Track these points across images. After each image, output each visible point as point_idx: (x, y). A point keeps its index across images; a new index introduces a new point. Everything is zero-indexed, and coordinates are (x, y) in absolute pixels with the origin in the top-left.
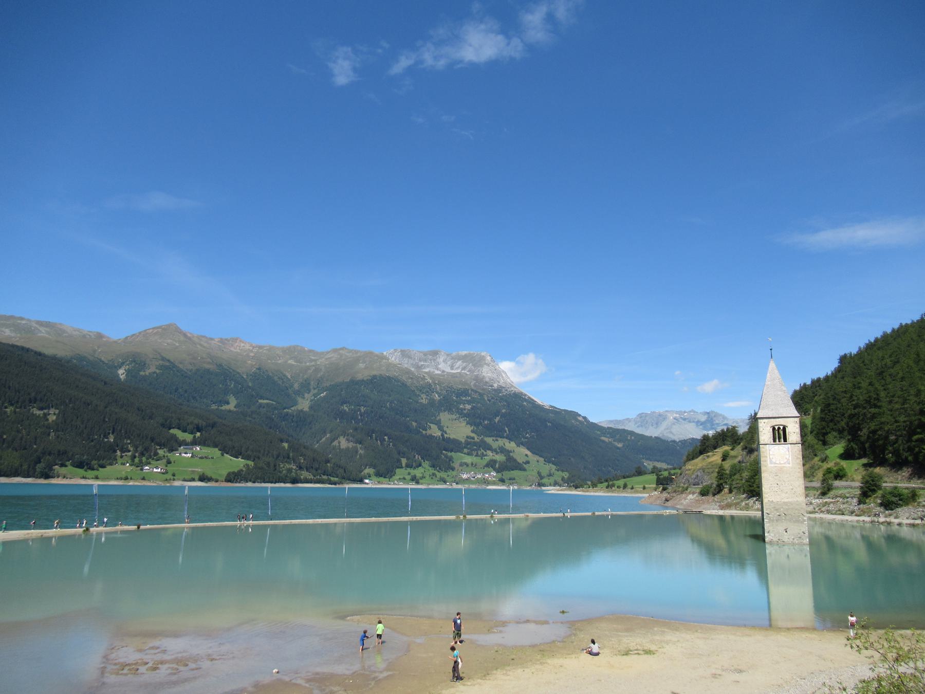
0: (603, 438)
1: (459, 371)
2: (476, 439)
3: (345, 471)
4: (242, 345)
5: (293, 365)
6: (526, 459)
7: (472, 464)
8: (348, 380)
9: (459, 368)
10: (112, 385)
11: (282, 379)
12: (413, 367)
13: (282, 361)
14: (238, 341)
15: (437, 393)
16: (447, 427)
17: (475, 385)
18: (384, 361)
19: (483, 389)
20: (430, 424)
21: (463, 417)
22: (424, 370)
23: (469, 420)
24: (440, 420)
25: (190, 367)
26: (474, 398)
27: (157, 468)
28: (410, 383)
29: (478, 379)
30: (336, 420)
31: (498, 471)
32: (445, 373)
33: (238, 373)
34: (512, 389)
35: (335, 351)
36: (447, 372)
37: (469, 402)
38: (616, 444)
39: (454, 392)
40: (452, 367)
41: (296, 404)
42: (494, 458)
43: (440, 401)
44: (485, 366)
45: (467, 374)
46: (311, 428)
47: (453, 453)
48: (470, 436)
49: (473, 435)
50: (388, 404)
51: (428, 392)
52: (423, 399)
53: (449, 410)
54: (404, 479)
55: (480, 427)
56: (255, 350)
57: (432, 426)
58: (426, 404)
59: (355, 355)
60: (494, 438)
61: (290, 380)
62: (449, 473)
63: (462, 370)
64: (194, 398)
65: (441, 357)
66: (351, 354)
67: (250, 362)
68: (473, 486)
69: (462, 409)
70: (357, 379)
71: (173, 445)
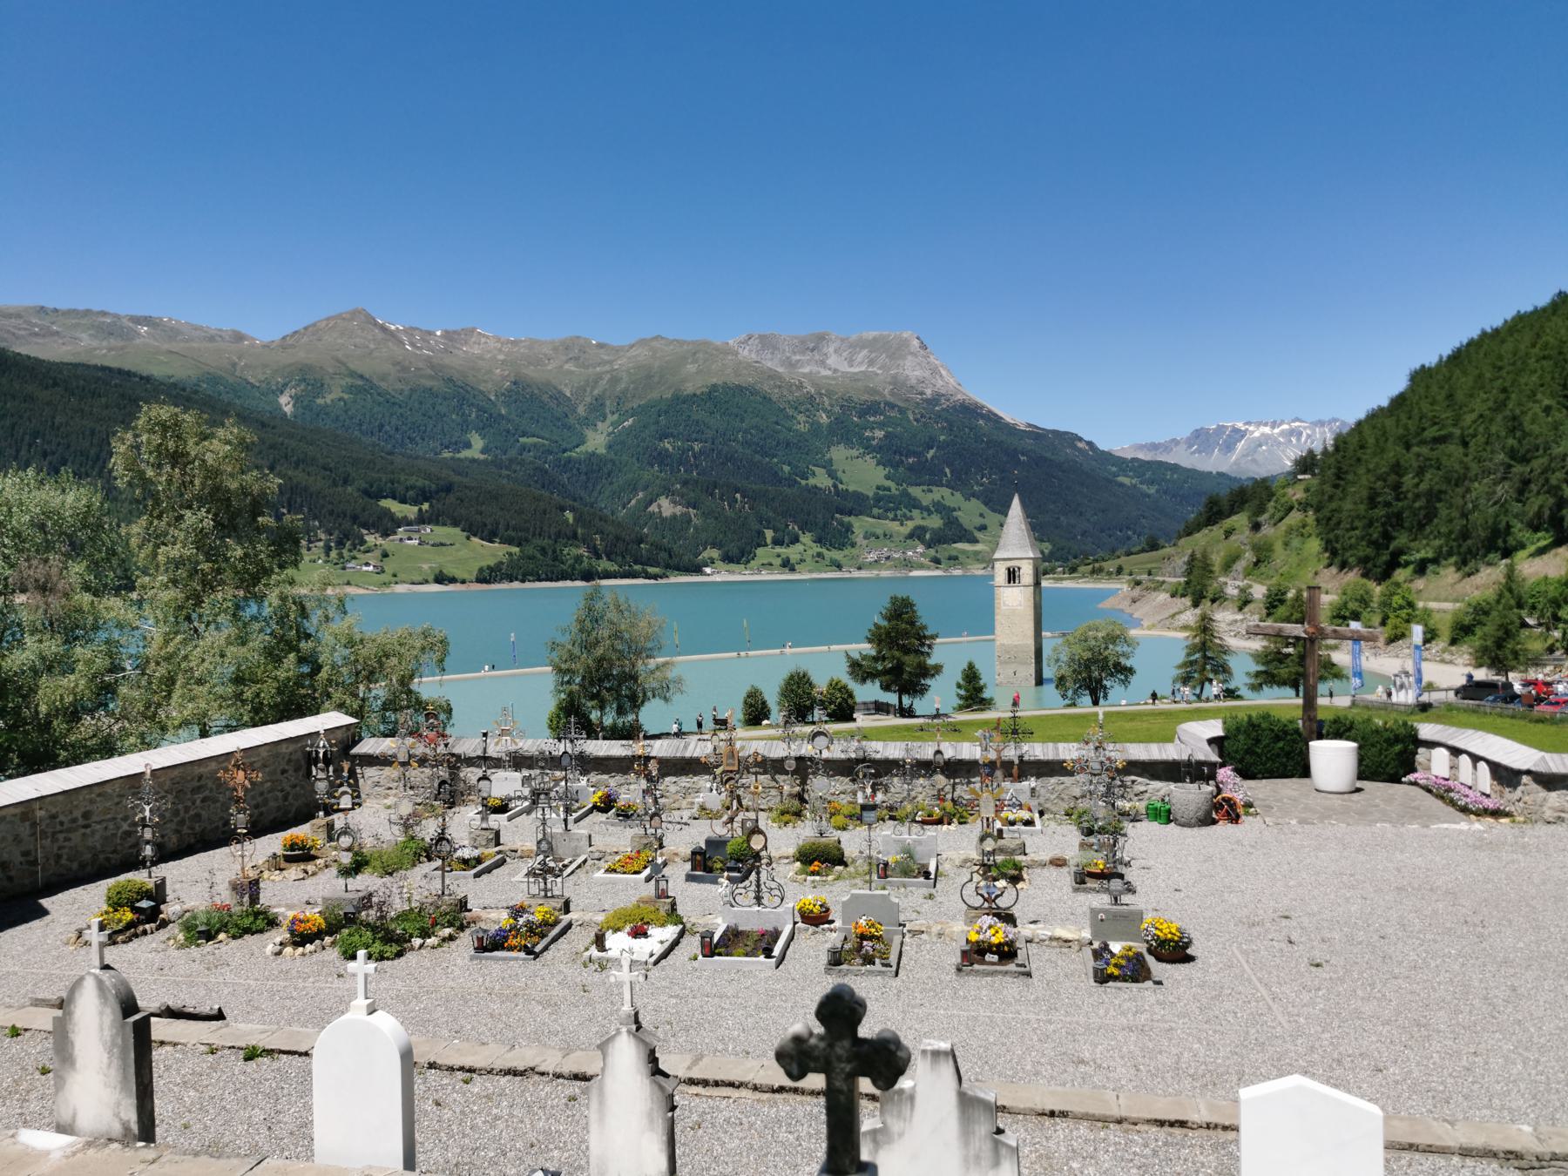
0: (1121, 479)
1: (863, 368)
2: (893, 490)
3: (670, 556)
4: (483, 340)
5: (572, 372)
6: (978, 521)
7: (885, 535)
10: (274, 428)
15: (825, 410)
17: (892, 393)
24: (831, 460)
25: (399, 386)
27: (367, 564)
29: (896, 382)
31: (928, 546)
33: (481, 392)
34: (959, 397)
35: (643, 342)
37: (881, 426)
38: (1144, 487)
40: (851, 363)
41: (582, 442)
42: (922, 523)
44: (910, 357)
45: (877, 374)
49: (888, 483)
53: (849, 443)
54: (771, 565)
55: (901, 469)
57: (816, 469)
60: (925, 488)
62: (846, 552)
64: (411, 440)
68: (885, 573)
69: (868, 439)
71: (387, 524)
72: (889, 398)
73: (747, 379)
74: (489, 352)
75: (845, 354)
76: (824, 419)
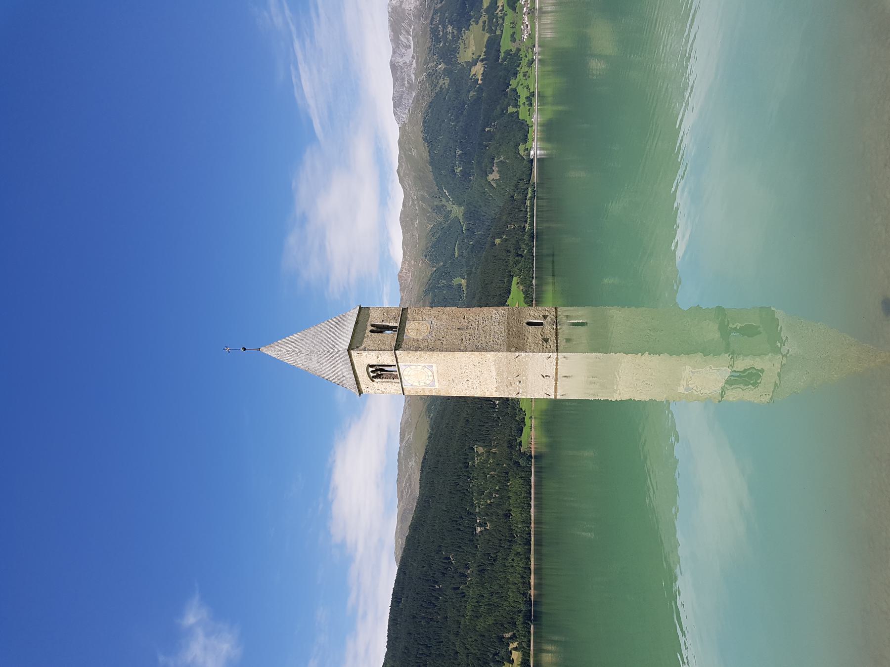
1: (411, 38)
4: (404, 271)
8: (430, 167)
9: (408, 39)
13: (416, 233)
14: (401, 275)
15: (436, 66)
16: (473, 54)
18: (407, 128)
19: (430, 8)
20: (471, 75)
21: (461, 34)
26: (439, 21)
28: (428, 98)
29: (418, 16)
30: (470, 180)
32: (415, 54)
36: (414, 52)
37: (445, 27)
39: (434, 46)
43: (445, 63)
44: (403, 6)
46: (480, 206)
47: (501, 50)
48: (483, 26)
51: (436, 77)
52: (445, 83)
53: (455, 51)
55: (472, 13)
58: (450, 80)
61: (434, 226)
62: (523, 56)
63: (410, 35)
66: (403, 164)
69: (453, 37)
70: (428, 158)
72: (429, 21)
73: (420, 116)
74: (411, 268)
75: (403, 51)
76: (442, 66)
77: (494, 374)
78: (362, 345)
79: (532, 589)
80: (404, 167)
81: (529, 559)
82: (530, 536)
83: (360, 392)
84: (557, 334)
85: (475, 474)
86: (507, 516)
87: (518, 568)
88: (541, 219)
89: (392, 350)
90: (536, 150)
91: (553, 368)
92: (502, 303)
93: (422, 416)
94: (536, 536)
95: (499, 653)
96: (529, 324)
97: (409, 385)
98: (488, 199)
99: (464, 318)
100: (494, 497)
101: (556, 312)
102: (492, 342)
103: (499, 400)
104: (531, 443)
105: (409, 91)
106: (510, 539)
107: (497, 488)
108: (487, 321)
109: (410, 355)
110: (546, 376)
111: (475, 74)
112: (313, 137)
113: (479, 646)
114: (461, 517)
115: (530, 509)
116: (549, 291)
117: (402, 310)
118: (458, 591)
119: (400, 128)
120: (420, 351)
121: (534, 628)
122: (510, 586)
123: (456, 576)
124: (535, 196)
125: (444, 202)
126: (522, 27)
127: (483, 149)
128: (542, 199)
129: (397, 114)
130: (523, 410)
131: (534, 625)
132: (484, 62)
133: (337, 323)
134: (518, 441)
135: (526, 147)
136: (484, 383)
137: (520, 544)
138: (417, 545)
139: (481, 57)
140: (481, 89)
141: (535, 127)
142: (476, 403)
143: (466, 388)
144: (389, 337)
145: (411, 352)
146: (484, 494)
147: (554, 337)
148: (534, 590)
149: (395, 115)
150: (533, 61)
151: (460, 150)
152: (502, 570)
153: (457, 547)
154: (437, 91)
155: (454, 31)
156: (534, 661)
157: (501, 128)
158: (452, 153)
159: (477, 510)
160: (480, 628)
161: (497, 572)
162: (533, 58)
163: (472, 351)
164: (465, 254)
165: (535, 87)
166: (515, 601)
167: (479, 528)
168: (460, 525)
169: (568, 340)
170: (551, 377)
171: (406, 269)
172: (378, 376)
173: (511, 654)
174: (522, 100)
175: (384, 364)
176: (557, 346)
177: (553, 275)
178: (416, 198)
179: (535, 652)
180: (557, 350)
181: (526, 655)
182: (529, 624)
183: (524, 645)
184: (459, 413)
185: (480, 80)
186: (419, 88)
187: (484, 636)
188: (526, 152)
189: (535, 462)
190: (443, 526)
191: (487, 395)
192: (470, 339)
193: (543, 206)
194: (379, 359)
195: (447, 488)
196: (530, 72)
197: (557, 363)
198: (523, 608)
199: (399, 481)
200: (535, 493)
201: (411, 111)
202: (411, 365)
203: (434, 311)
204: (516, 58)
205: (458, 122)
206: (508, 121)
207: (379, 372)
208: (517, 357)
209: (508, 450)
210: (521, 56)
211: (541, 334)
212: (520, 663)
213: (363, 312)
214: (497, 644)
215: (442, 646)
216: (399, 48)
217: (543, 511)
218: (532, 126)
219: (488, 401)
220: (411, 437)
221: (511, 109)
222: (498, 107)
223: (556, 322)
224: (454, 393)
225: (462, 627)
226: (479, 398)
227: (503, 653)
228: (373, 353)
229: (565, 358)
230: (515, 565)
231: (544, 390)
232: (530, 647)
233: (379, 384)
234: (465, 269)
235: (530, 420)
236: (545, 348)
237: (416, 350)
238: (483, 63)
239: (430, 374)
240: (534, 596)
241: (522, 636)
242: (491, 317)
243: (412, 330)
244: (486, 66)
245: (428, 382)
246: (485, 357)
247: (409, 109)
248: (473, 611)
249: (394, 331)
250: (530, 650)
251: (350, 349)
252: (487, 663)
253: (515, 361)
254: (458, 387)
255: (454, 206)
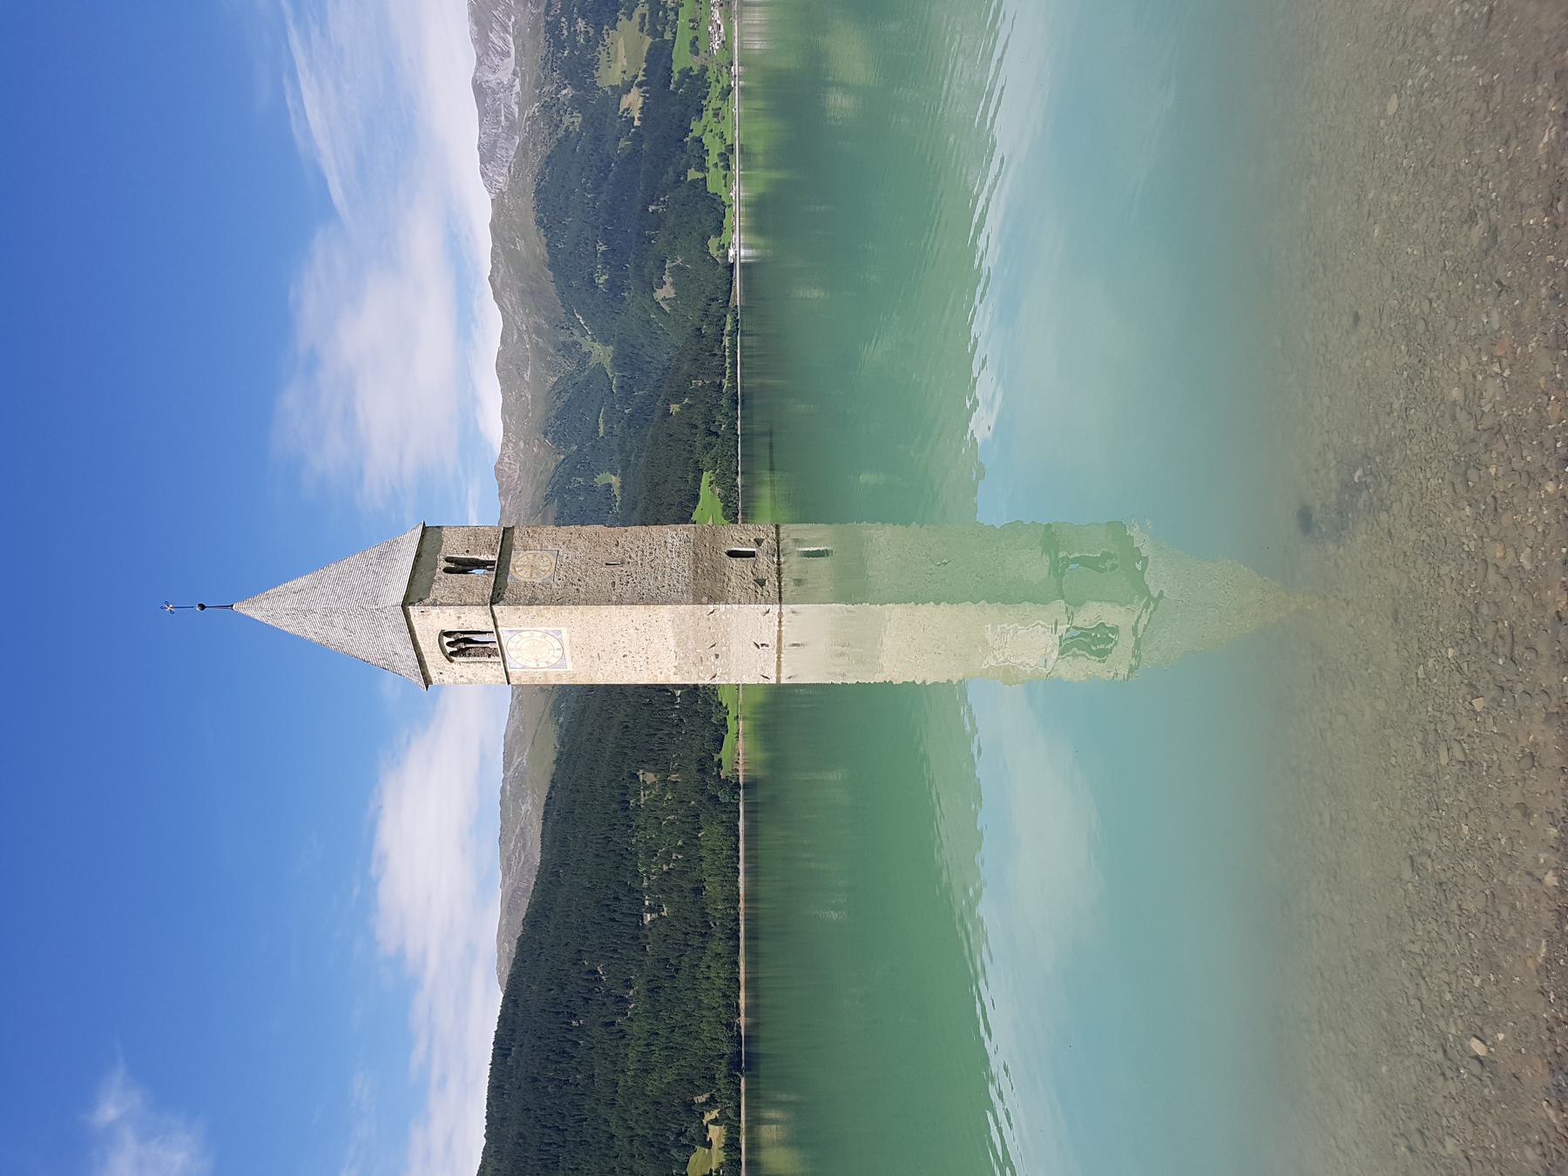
4: (506, 460)
5: (531, 372)
7: (693, 28)
11: (560, 393)
12: (513, 138)
14: (501, 468)
15: (558, 91)
16: (624, 72)
17: (537, 5)
20: (621, 110)
21: (601, 35)
22: (517, 116)
23: (607, 24)
30: (624, 298)
32: (518, 68)
33: (557, 468)
35: (497, 296)
36: (516, 65)
37: (572, 22)
43: (574, 87)
47: (673, 68)
48: (640, 23)
50: (589, 196)
51: (558, 111)
53: (592, 65)
56: (513, 438)
58: (584, 118)
59: (502, 258)
62: (712, 80)
63: (509, 34)
65: (485, 79)
66: (500, 266)
67: (534, 449)
69: (588, 40)
70: (547, 255)
72: (542, 9)
75: (497, 60)
77: (672, 642)
78: (428, 597)
79: (743, 1015)
80: (502, 271)
81: (736, 964)
82: (738, 924)
83: (427, 681)
84: (779, 572)
85: (640, 821)
86: (698, 891)
87: (718, 982)
88: (750, 371)
89: (486, 604)
90: (739, 250)
91: (774, 631)
92: (685, 518)
93: (543, 721)
94: (748, 922)
95: (686, 1131)
96: (732, 554)
97: (518, 666)
98: (656, 333)
99: (617, 545)
100: (674, 860)
101: (778, 534)
102: (667, 587)
103: (683, 689)
104: (737, 763)
105: (508, 134)
106: (703, 932)
107: (680, 843)
108: (657, 550)
109: (519, 613)
110: (762, 645)
111: (627, 109)
112: (327, 210)
113: (651, 1121)
114: (617, 899)
115: (737, 877)
116: (765, 497)
117: (504, 532)
118: (612, 1028)
119: (492, 200)
120: (537, 605)
121: (746, 1083)
122: (704, 1013)
123: (608, 1001)
124: (738, 329)
125: (577, 336)
126: (710, 28)
127: (644, 243)
128: (752, 335)
129: (487, 175)
130: (724, 705)
131: (746, 1077)
132: (644, 88)
133: (381, 555)
134: (716, 759)
135: (721, 243)
136: (654, 660)
137: (720, 939)
138: (537, 952)
139: (639, 79)
140: (638, 136)
141: (736, 208)
142: (641, 695)
143: (623, 667)
144: (481, 580)
145: (520, 607)
146: (656, 855)
147: (775, 576)
148: (746, 1016)
149: (483, 177)
150: (730, 90)
151: (605, 244)
152: (689, 986)
153: (610, 950)
154: (559, 136)
155: (589, 29)
156: (746, 1140)
157: (676, 206)
158: (589, 248)
159: (645, 884)
160: (652, 1091)
161: (681, 991)
162: (730, 85)
163: (633, 604)
164: (617, 431)
165: (735, 137)
166: (712, 1039)
167: (649, 915)
168: (615, 911)
169: (799, 582)
170: (770, 647)
171: (509, 456)
172: (461, 652)
173: (707, 1131)
174: (712, 158)
175: (471, 629)
176: (780, 592)
177: (772, 469)
178: (525, 329)
179: (749, 1124)
180: (780, 598)
181: (733, 1130)
182: (737, 1076)
183: (730, 1113)
184: (612, 713)
185: (636, 119)
186: (527, 128)
187: (660, 1103)
188: (721, 251)
189: (744, 795)
190: (584, 915)
191: (661, 680)
192: (628, 582)
193: (751, 347)
194: (461, 621)
195: (591, 848)
196: (725, 109)
197: (780, 622)
198: (727, 1049)
199: (503, 840)
200: (746, 850)
201: (512, 169)
202: (522, 631)
203: (563, 532)
204: (700, 83)
205: (599, 194)
206: (688, 196)
207: (461, 644)
208: (711, 613)
209: (698, 777)
210: (709, 80)
211: (752, 572)
212: (722, 1145)
213: (430, 535)
214: (683, 1115)
215: (584, 1127)
216: (488, 55)
217: (761, 878)
218: (730, 206)
219: (662, 689)
220: (524, 761)
221: (693, 174)
222: (670, 170)
223: (778, 551)
224: (600, 680)
225: (619, 1091)
226: (646, 686)
227: (693, 1130)
228: (451, 611)
229: (793, 612)
230: (712, 975)
231: (759, 669)
232: (740, 1116)
233: (464, 669)
234: (617, 457)
235: (736, 722)
236: (759, 596)
237: (530, 604)
238: (642, 90)
239: (557, 645)
240: (746, 1027)
241: (727, 1098)
242: (666, 542)
243: (522, 567)
244: (647, 95)
245: (554, 661)
246: (656, 614)
247: (510, 167)
248: (639, 1061)
249: (489, 570)
250: (740, 1121)
251: (405, 605)
252: (665, 1150)
253: (709, 619)
254: (608, 668)
255: (595, 345)
